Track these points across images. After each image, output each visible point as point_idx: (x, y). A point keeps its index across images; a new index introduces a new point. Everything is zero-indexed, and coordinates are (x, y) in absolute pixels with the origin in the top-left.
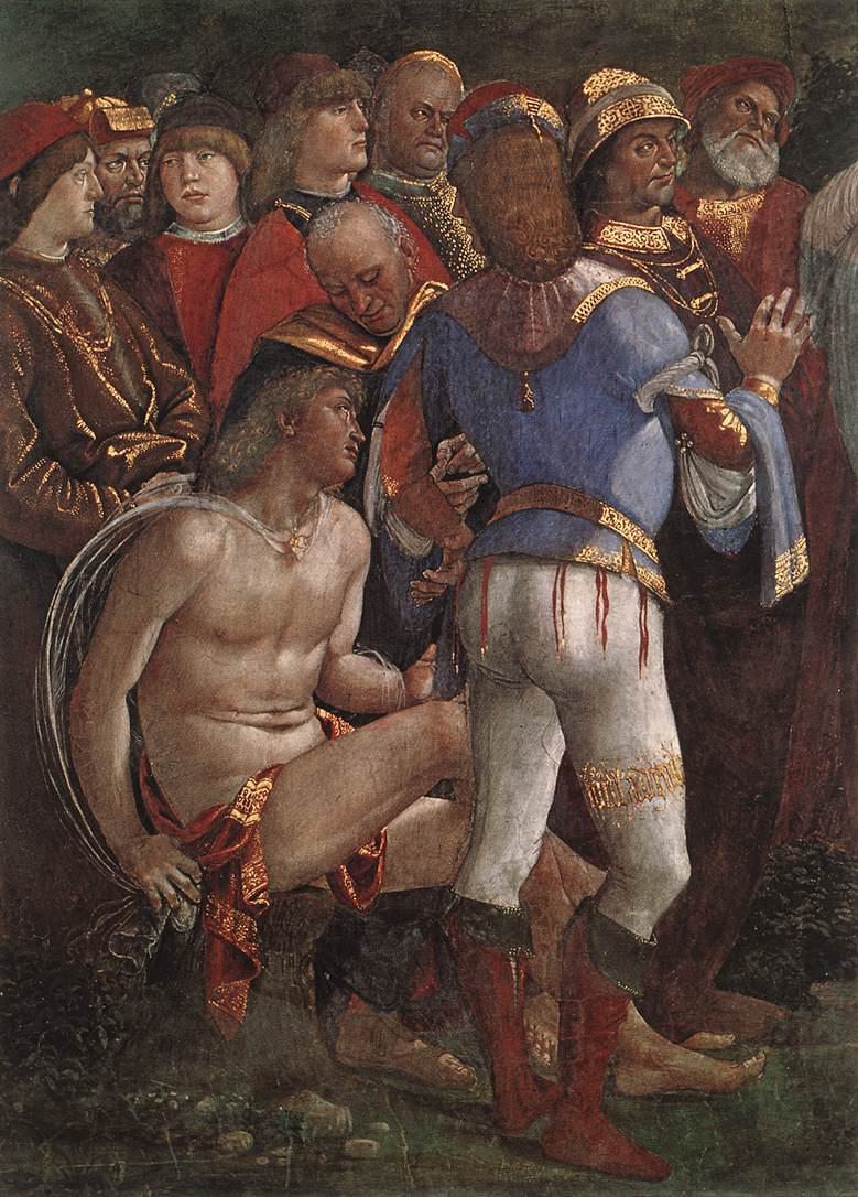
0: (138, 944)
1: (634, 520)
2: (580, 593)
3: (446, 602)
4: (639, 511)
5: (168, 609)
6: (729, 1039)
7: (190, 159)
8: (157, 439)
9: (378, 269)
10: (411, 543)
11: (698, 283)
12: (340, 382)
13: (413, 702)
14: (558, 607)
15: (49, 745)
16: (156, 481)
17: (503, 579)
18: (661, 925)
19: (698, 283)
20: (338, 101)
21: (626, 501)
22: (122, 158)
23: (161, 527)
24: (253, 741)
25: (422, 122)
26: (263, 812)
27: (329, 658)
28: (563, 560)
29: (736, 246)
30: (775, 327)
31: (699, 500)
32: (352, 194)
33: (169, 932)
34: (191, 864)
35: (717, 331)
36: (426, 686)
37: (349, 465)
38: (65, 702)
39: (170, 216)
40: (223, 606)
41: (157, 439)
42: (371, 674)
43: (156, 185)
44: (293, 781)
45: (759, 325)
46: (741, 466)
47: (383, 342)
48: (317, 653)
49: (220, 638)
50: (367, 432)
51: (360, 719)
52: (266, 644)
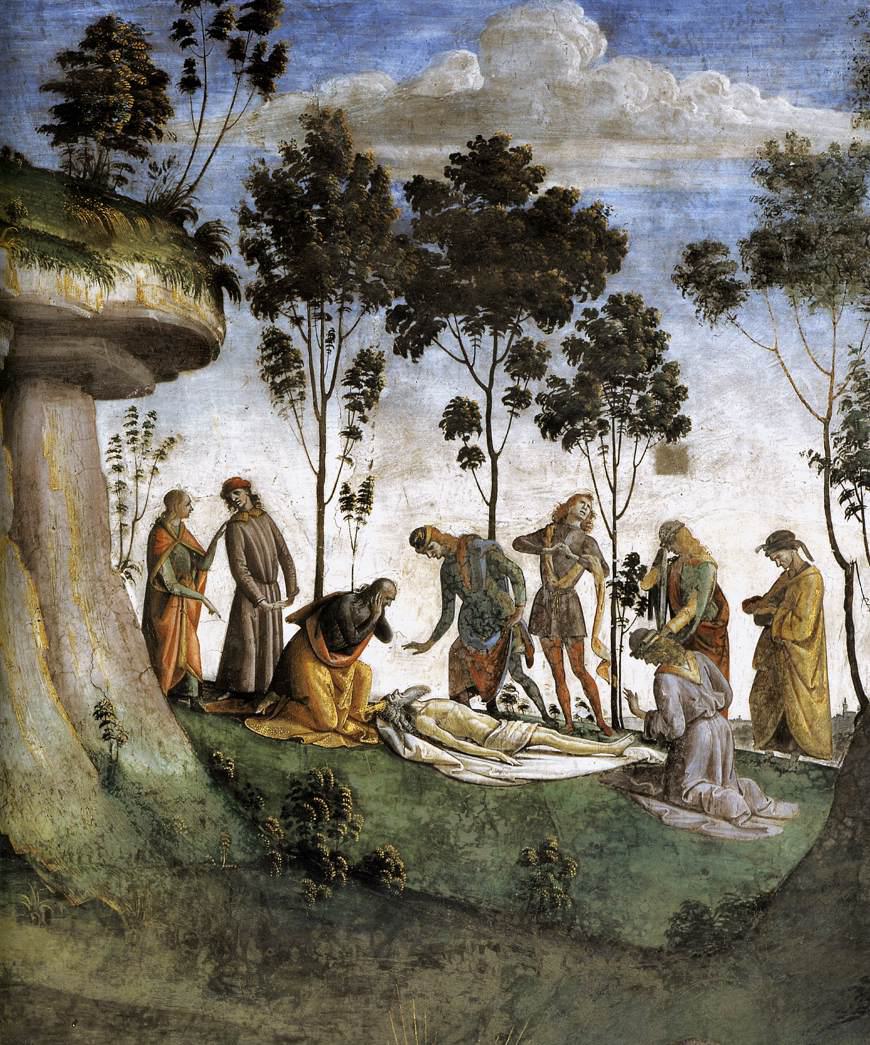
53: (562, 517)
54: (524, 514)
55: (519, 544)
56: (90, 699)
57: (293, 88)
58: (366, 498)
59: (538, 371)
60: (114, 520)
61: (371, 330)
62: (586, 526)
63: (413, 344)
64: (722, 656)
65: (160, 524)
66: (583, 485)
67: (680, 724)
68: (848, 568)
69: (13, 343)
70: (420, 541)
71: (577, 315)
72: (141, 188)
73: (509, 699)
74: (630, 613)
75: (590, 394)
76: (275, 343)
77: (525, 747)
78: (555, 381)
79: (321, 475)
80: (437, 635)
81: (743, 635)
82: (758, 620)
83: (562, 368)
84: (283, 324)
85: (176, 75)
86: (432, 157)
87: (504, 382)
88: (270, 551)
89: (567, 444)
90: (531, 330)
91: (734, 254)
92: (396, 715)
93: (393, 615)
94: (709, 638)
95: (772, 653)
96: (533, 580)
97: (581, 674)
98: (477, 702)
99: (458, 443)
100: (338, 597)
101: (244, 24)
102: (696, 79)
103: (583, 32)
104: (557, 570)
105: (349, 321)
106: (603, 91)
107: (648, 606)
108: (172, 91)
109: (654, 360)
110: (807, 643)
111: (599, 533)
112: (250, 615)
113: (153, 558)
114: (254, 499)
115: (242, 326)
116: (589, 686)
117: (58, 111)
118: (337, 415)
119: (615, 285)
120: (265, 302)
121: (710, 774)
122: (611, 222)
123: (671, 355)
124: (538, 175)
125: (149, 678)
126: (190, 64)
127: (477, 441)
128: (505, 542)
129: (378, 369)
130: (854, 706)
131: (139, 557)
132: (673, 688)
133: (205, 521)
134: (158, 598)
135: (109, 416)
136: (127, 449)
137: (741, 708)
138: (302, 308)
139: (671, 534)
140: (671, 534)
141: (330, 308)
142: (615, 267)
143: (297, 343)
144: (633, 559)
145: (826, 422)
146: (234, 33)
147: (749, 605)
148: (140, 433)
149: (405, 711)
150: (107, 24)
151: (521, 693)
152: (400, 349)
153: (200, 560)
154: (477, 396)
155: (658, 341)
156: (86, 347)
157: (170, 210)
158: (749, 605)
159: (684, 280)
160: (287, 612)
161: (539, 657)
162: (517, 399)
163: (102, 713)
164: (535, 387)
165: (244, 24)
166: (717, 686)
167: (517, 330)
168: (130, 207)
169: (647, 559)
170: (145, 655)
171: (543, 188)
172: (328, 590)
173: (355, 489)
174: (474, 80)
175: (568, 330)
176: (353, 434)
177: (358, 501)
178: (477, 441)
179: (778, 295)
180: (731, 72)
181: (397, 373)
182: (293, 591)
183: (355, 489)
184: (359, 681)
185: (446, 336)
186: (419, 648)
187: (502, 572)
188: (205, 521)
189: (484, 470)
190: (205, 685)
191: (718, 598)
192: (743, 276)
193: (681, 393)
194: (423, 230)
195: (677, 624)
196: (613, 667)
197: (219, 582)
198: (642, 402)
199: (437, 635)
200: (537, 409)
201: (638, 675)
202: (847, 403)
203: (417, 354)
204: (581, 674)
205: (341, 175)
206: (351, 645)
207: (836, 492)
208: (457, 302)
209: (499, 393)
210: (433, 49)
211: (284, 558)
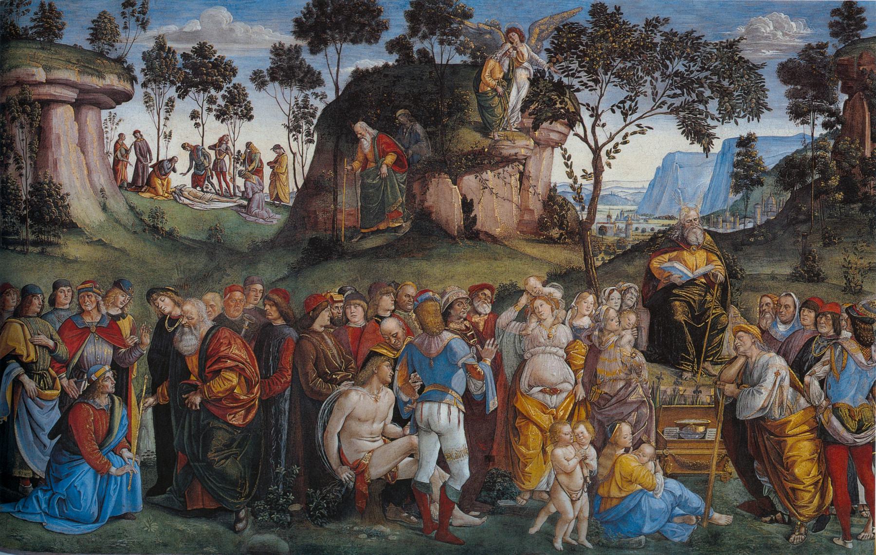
0: (340, 491)
1: (457, 393)
2: (444, 408)
3: (414, 411)
4: (458, 391)
5: (347, 414)
6: (477, 513)
7: (352, 307)
8: (345, 374)
9: (397, 333)
10: (405, 398)
11: (472, 336)
12: (388, 360)
13: (405, 435)
14: (439, 413)
15: (319, 446)
16: (345, 383)
17: (426, 406)
19: (472, 336)
20: (387, 293)
21: (455, 388)
22: (337, 307)
23: (346, 393)
24: (367, 445)
25: (408, 299)
26: (369, 461)
27: (385, 425)
28: (440, 402)
29: (481, 328)
30: (490, 347)
31: (472, 388)
32: (391, 316)
33: (347, 488)
34: (352, 473)
35: (477, 349)
36: (408, 432)
39: (348, 320)
40: (360, 412)
41: (345, 374)
42: (396, 429)
43: (345, 313)
44: (376, 454)
45: (486, 347)
46: (482, 380)
47: (398, 351)
48: (382, 425)
50: (394, 372)
51: (392, 440)
53: (221, 140)
54: (211, 139)
55: (210, 148)
56: (99, 189)
57: (151, 29)
58: (170, 136)
59: (215, 103)
60: (105, 140)
61: (171, 92)
62: (227, 143)
63: (182, 96)
64: (262, 178)
65: (117, 142)
66: (227, 133)
67: (251, 195)
68: (294, 154)
69: (78, 95)
70: (184, 147)
71: (225, 88)
72: (113, 55)
73: (207, 188)
74: (238, 165)
75: (228, 109)
76: (147, 95)
77: (211, 200)
78: (219, 106)
79: (159, 130)
80: (188, 171)
81: (267, 171)
82: (271, 168)
83: (221, 102)
84: (149, 90)
85: (122, 26)
86: (187, 47)
87: (206, 106)
88: (145, 149)
89: (222, 122)
90: (213, 92)
91: (265, 73)
92: (177, 191)
93: (177, 166)
94: (258, 171)
95: (275, 176)
96: (213, 158)
97: (225, 181)
98: (198, 188)
99: (194, 122)
100: (163, 161)
101: (139, 13)
102: (256, 28)
103: (226, 15)
104: (219, 153)
105: (166, 89)
106: (232, 30)
107: (243, 163)
108: (120, 30)
109: (245, 100)
110: (283, 174)
111: (230, 144)
112: (140, 166)
113: (115, 151)
114: (141, 135)
115: (139, 91)
116: (228, 185)
117: (92, 35)
118: (163, 114)
119: (235, 80)
120: (144, 85)
121: (258, 207)
122: (233, 65)
123: (248, 99)
124: (215, 52)
125: (114, 182)
126: (125, 22)
127: (199, 121)
128: (206, 147)
129: (173, 102)
130: (296, 190)
131: (112, 150)
132: (249, 184)
133: (129, 141)
134: (116, 161)
135: (105, 114)
136: (109, 123)
137: (266, 190)
138: (154, 86)
139: (248, 145)
140: (248, 145)
141: (161, 86)
142: (234, 75)
143: (153, 96)
144: (239, 152)
145: (289, 116)
146: (137, 15)
147: (268, 164)
148: (112, 118)
149: (180, 191)
150: (104, 12)
151: (210, 186)
152: (179, 97)
153: (127, 151)
154: (200, 110)
155: (246, 95)
156: (97, 96)
157: (120, 60)
158: (268, 164)
159: (253, 80)
160: (150, 165)
161: (215, 177)
162: (209, 110)
163: (102, 191)
164: (214, 107)
165: (139, 13)
166: (260, 184)
167: (209, 92)
168: (109, 59)
169: (243, 152)
170: (113, 176)
171: (216, 56)
172: (160, 159)
173: (167, 133)
174: (199, 28)
175: (223, 92)
176: (167, 119)
177: (168, 136)
178: (199, 121)
179: (277, 84)
180: (264, 25)
181: (178, 103)
182: (151, 160)
183: (167, 133)
184: (168, 183)
185: (190, 93)
186: (185, 174)
187: (206, 156)
188: (129, 141)
189: (201, 127)
190: (128, 184)
191: (261, 161)
192: (268, 79)
193: (251, 109)
194: (185, 66)
195: (250, 169)
196: (233, 179)
197: (133, 158)
198: (242, 111)
199: (188, 171)
200: (214, 113)
201: (240, 182)
202: (293, 112)
203: (183, 98)
204: (225, 181)
205: (164, 52)
206: (166, 174)
207: (291, 135)
208: (196, 85)
209: (205, 108)
210: (188, 19)
211: (149, 151)
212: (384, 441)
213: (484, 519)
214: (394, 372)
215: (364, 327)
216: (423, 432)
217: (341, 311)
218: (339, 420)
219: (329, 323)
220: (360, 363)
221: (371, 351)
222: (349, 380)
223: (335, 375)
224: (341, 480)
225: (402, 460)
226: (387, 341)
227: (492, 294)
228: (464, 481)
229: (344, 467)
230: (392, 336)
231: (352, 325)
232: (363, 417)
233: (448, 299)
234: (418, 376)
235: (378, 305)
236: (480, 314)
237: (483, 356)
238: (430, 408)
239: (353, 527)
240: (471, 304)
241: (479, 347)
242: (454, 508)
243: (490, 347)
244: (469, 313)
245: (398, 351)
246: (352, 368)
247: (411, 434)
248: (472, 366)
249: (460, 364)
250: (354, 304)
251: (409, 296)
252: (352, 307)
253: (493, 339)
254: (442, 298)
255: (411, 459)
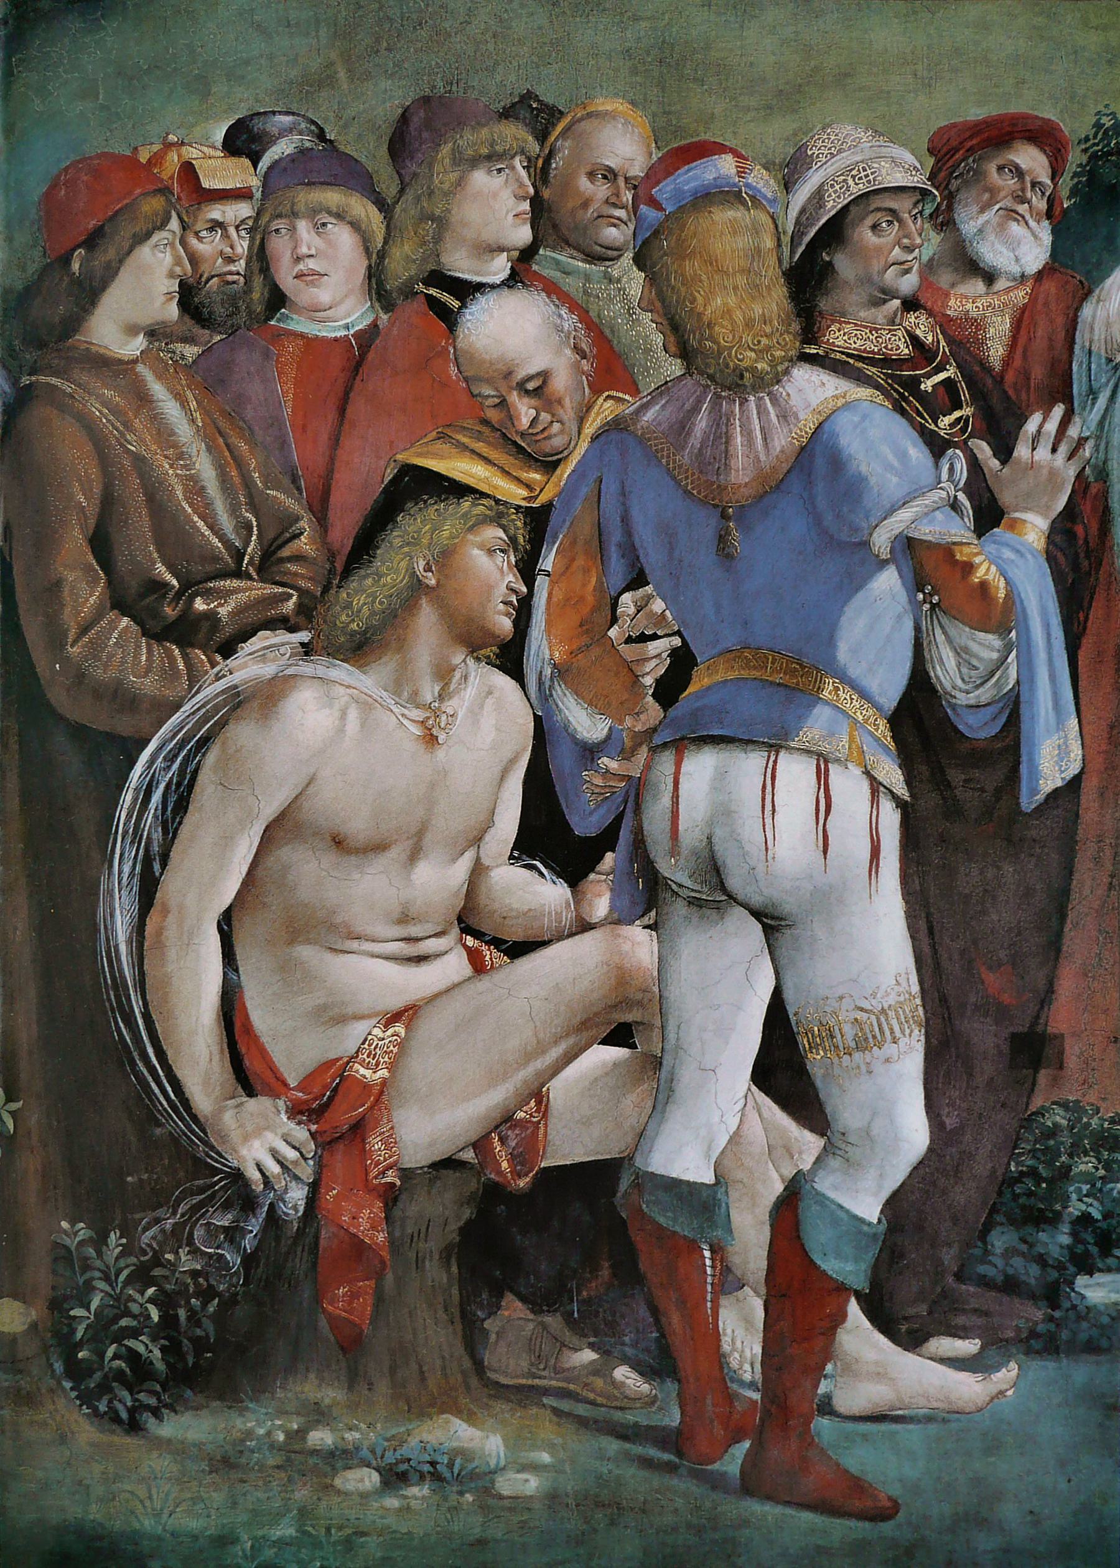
0: (233, 1234)
1: (864, 695)
4: (873, 685)
5: (269, 810)
6: (969, 1347)
7: (303, 227)
9: (545, 376)
13: (584, 926)
15: (119, 985)
18: (893, 1204)
20: (493, 158)
25: (600, 190)
26: (392, 1067)
27: (478, 871)
29: (996, 352)
30: (1043, 453)
32: (514, 280)
33: (273, 1219)
34: (301, 1134)
35: (974, 464)
36: (601, 906)
37: (505, 625)
38: (139, 929)
39: (277, 300)
43: (261, 258)
44: (432, 1026)
45: (1022, 451)
46: (1002, 629)
47: (550, 466)
48: (461, 869)
49: (339, 843)
50: (529, 581)
51: (518, 950)
52: (397, 853)
212: (478, 966)
213: (1006, 1375)
214: (529, 581)
215: (368, 337)
216: (679, 909)
217: (242, 246)
218: (227, 841)
219: (173, 311)
220: (344, 530)
221: (407, 469)
222: (286, 624)
223: (207, 594)
224: (237, 1176)
225: (570, 1057)
226: (493, 415)
227: (1055, 175)
228: (897, 1175)
229: (252, 1104)
230: (521, 386)
231: (299, 324)
232: (358, 826)
233: (819, 196)
234: (658, 606)
235: (442, 223)
236: (990, 277)
237: (1006, 498)
238: (721, 777)
239: (301, 1433)
240: (944, 220)
241: (983, 449)
242: (842, 1316)
243: (1043, 453)
244: (929, 268)
245: (550, 466)
246: (298, 558)
247: (617, 919)
248: (947, 551)
249: (882, 540)
250: (313, 212)
251: (610, 175)
252: (303, 227)
253: (1058, 411)
254: (788, 185)
255: (616, 1053)
